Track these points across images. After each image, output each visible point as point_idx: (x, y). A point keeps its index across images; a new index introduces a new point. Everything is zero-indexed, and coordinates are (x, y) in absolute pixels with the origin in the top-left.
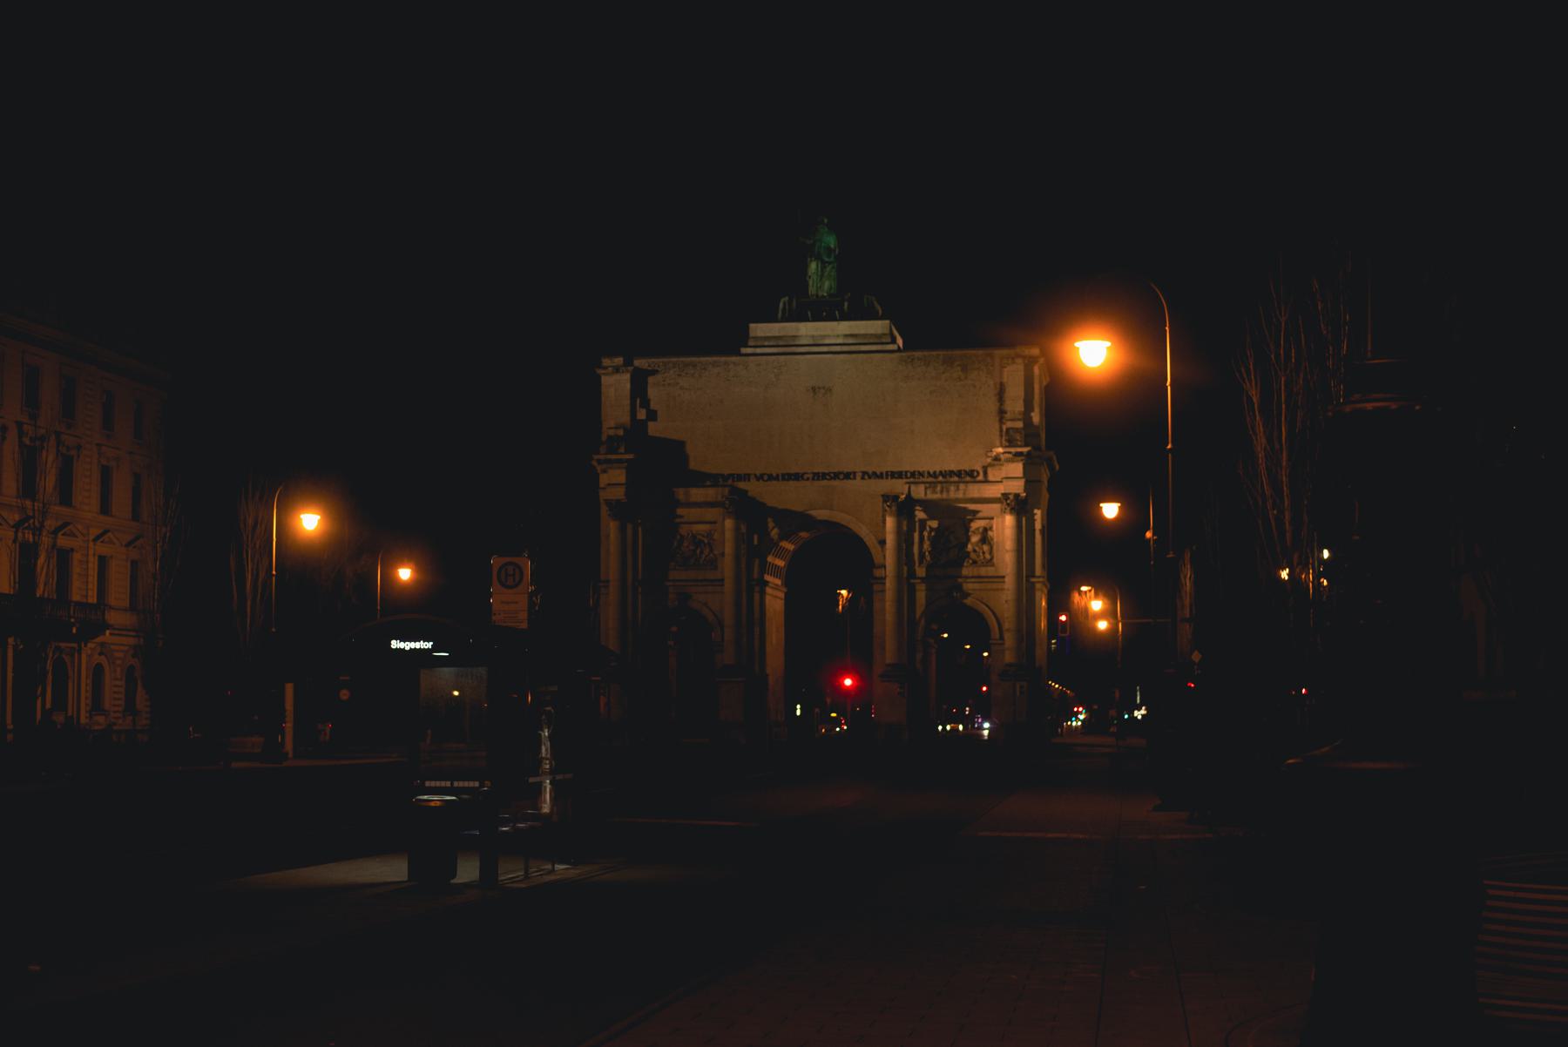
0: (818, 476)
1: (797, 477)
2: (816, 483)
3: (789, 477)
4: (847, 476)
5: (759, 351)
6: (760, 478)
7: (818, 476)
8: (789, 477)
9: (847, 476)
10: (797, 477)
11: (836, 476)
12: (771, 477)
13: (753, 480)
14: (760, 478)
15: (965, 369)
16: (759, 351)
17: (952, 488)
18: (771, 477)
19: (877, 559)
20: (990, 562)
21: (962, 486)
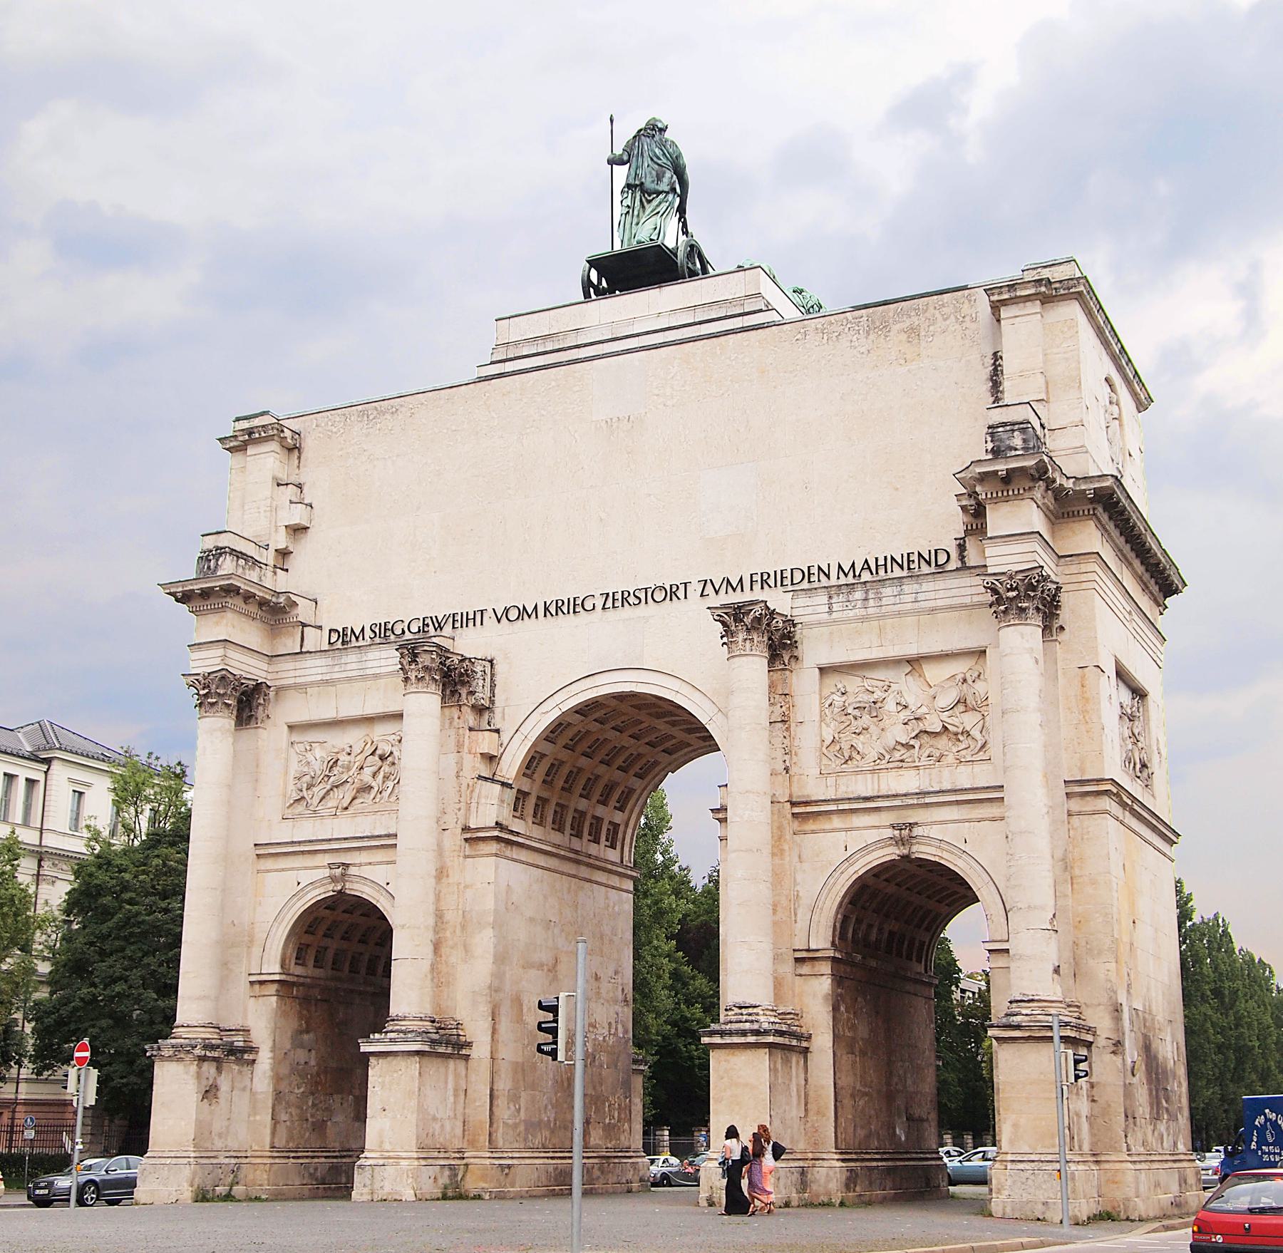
0: (616, 600)
1: (575, 606)
2: (611, 613)
3: (556, 609)
4: (671, 593)
5: (509, 367)
6: (502, 616)
7: (616, 600)
8: (556, 609)
9: (671, 593)
10: (575, 606)
11: (647, 595)
12: (523, 613)
13: (489, 619)
14: (502, 616)
15: (913, 332)
16: (509, 367)
17: (888, 591)
18: (523, 613)
21: (909, 587)
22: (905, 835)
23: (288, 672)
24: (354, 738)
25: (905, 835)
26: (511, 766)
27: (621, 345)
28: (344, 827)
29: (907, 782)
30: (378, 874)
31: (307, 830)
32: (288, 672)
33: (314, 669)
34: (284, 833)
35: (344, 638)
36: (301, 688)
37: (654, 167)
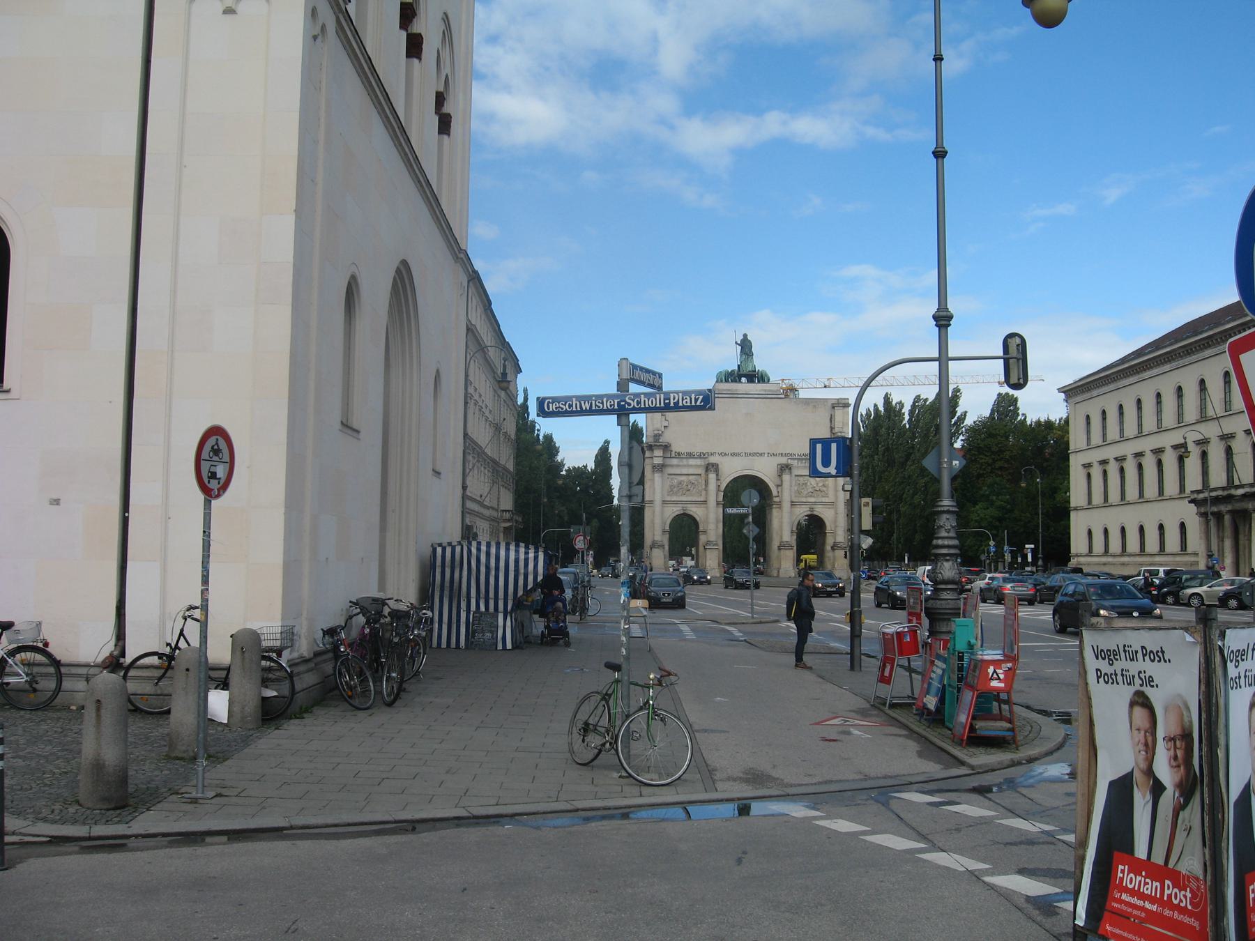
0: (747, 455)
1: (739, 455)
7: (747, 455)
10: (739, 455)
11: (755, 454)
19: (774, 492)
20: (827, 495)
22: (812, 509)
23: (669, 462)
24: (683, 478)
25: (812, 509)
26: (723, 488)
27: (747, 395)
28: (684, 498)
29: (812, 500)
30: (694, 509)
31: (674, 499)
32: (669, 462)
33: (675, 462)
34: (668, 499)
35: (679, 455)
36: (672, 466)
37: (746, 347)
